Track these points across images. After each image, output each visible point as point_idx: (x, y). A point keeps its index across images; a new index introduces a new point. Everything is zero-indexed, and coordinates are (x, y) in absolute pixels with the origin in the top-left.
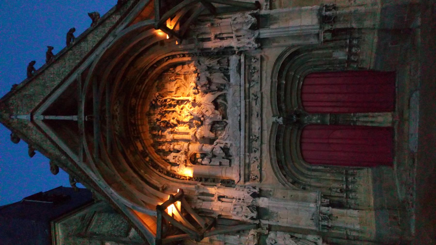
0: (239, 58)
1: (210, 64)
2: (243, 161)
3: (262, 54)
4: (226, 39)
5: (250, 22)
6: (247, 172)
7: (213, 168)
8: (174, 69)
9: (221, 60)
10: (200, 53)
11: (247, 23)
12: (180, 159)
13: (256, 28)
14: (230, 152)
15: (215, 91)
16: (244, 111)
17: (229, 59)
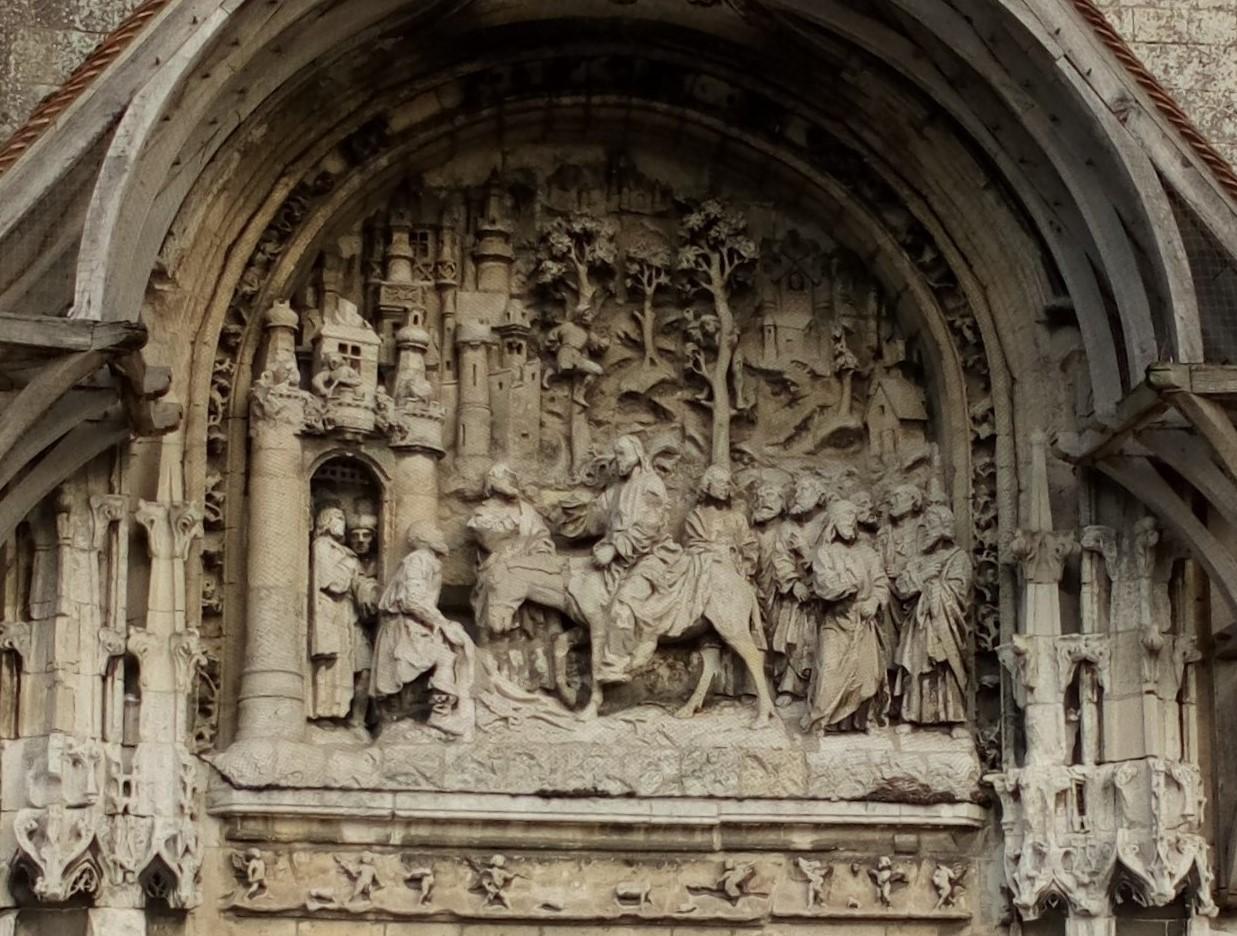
0: (962, 792)
1: (930, 614)
2: (355, 811)
3: (977, 926)
4: (1068, 722)
5: (1154, 867)
6: (285, 830)
7: (298, 614)
8: (900, 365)
9: (948, 678)
10: (994, 548)
11: (1147, 852)
12: (347, 397)
13: (1120, 900)
14: (406, 725)
15: (769, 634)
16: (655, 820)
17: (957, 732)
